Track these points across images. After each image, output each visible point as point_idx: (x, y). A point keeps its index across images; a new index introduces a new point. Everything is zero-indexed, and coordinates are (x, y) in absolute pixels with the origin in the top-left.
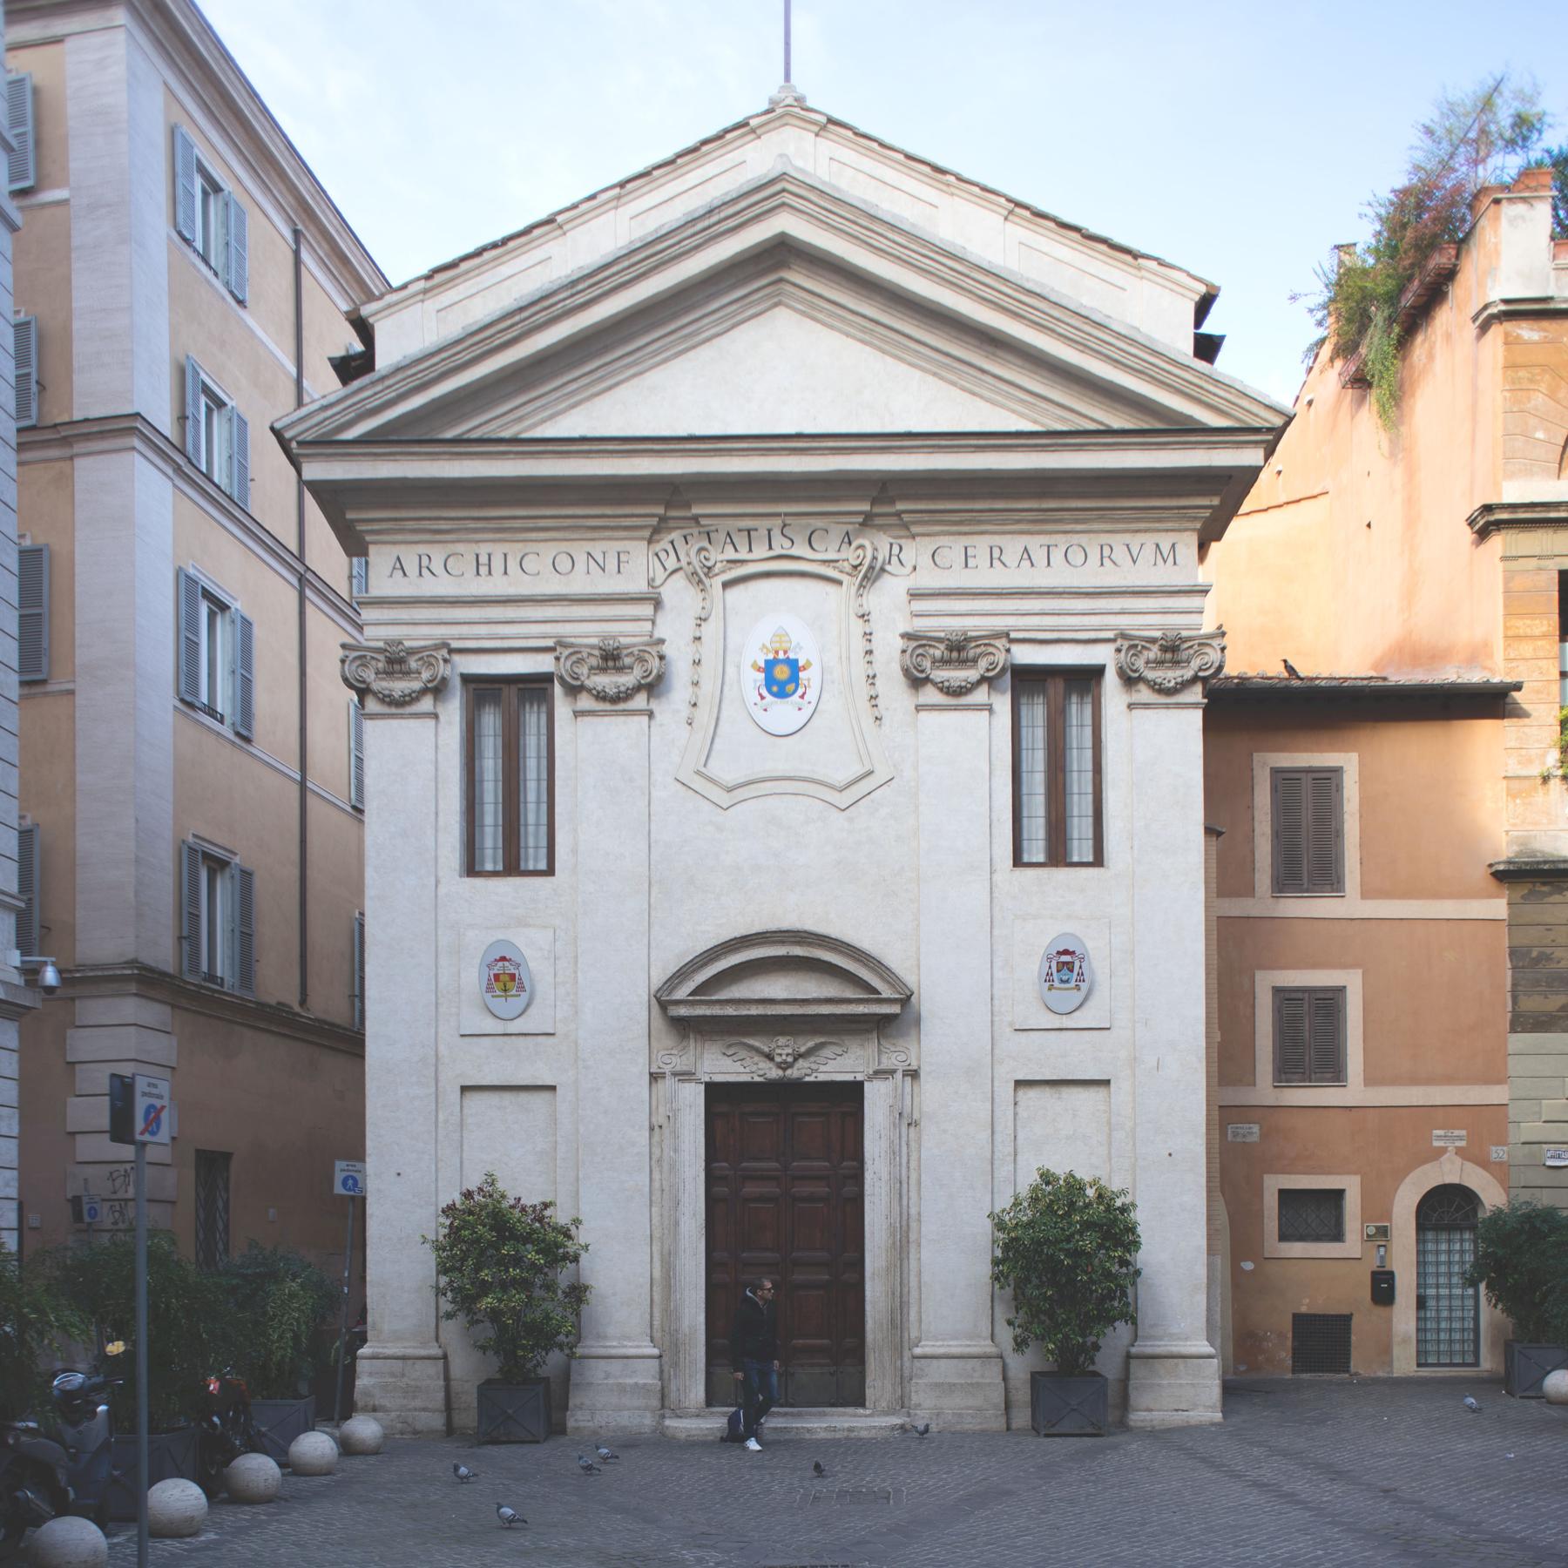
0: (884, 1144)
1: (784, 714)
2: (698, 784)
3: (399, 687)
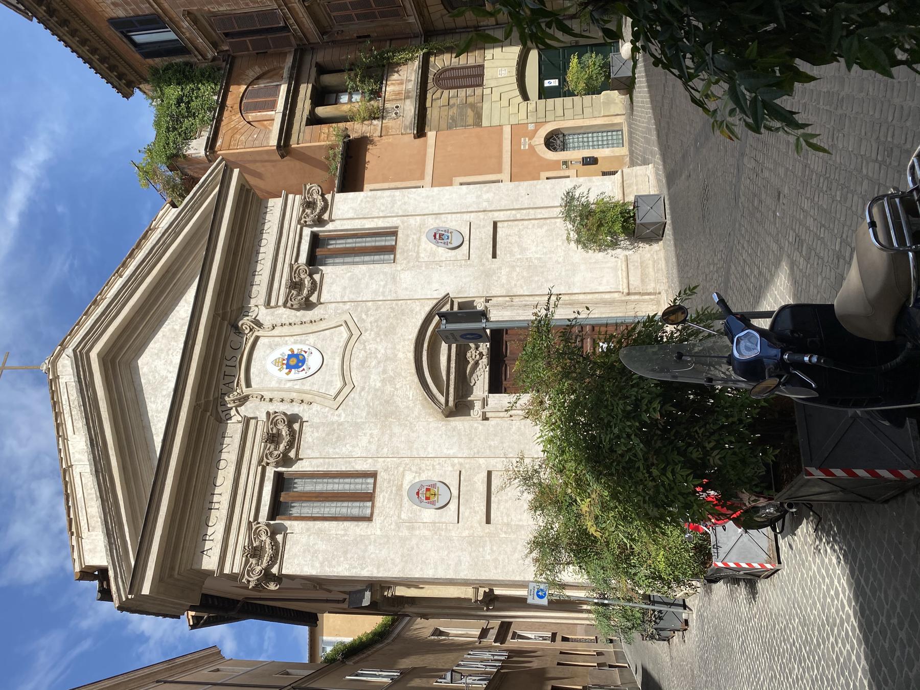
0: (521, 312)
1: (313, 361)
2: (340, 399)
3: (269, 551)
